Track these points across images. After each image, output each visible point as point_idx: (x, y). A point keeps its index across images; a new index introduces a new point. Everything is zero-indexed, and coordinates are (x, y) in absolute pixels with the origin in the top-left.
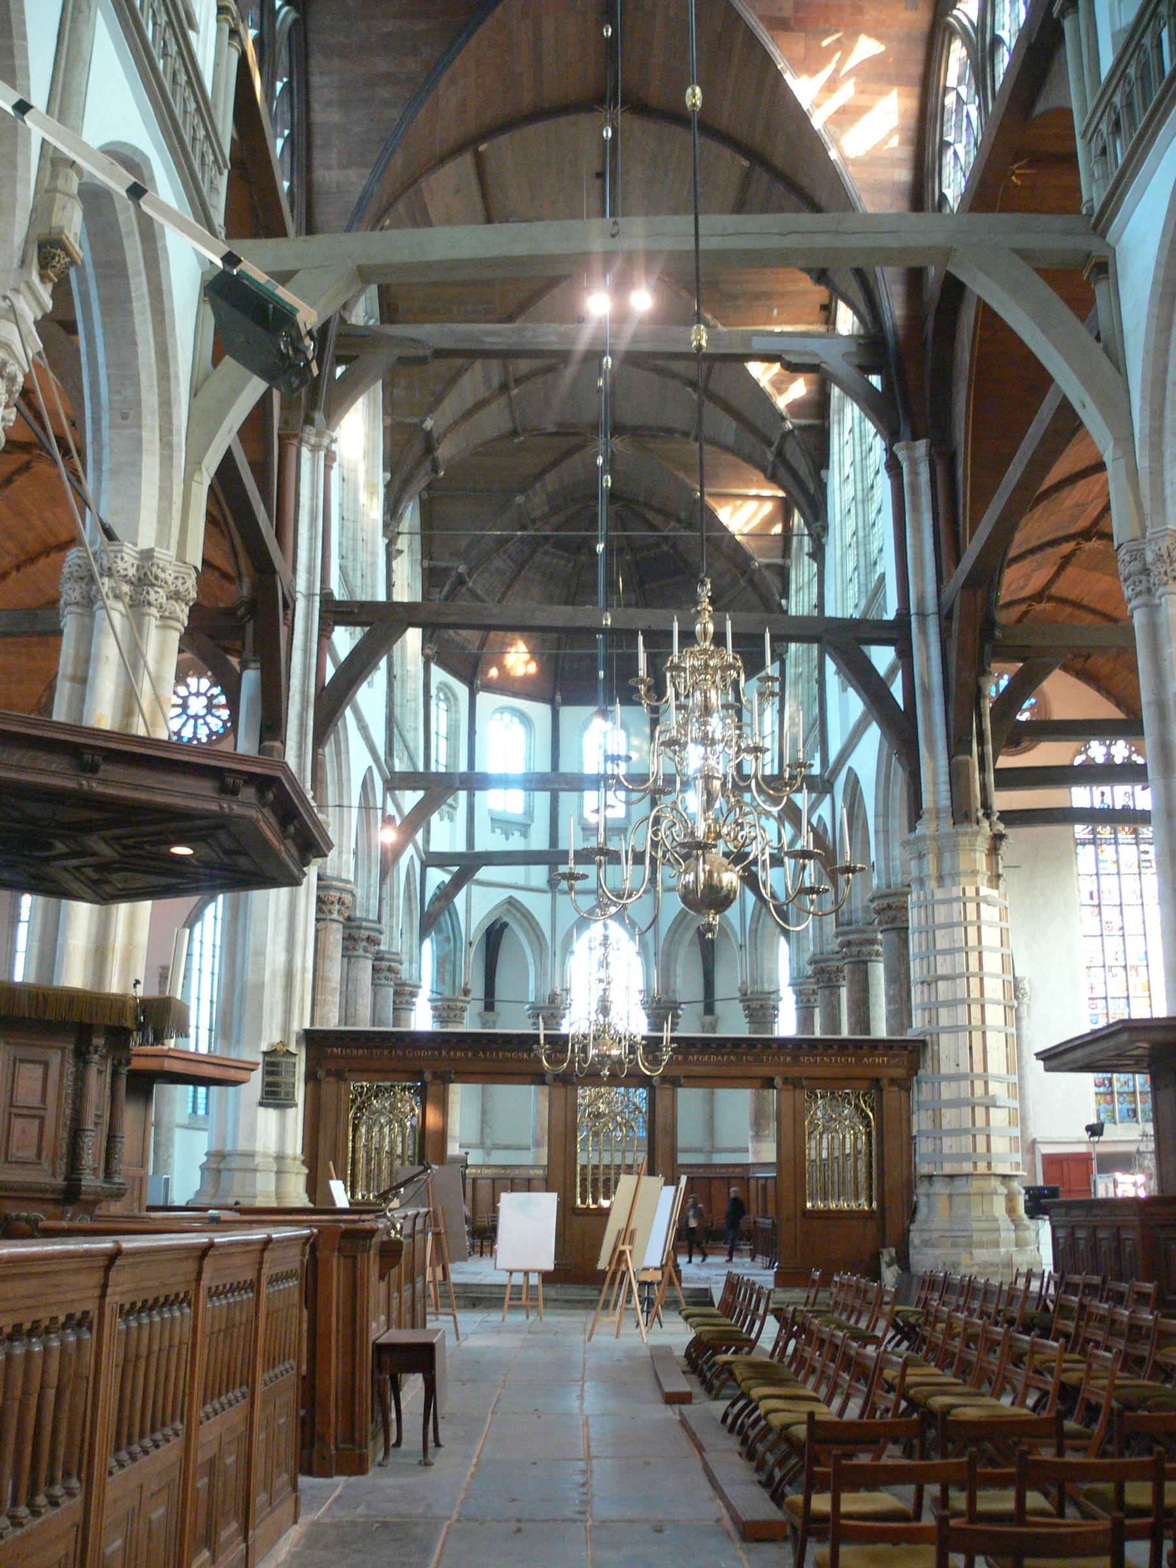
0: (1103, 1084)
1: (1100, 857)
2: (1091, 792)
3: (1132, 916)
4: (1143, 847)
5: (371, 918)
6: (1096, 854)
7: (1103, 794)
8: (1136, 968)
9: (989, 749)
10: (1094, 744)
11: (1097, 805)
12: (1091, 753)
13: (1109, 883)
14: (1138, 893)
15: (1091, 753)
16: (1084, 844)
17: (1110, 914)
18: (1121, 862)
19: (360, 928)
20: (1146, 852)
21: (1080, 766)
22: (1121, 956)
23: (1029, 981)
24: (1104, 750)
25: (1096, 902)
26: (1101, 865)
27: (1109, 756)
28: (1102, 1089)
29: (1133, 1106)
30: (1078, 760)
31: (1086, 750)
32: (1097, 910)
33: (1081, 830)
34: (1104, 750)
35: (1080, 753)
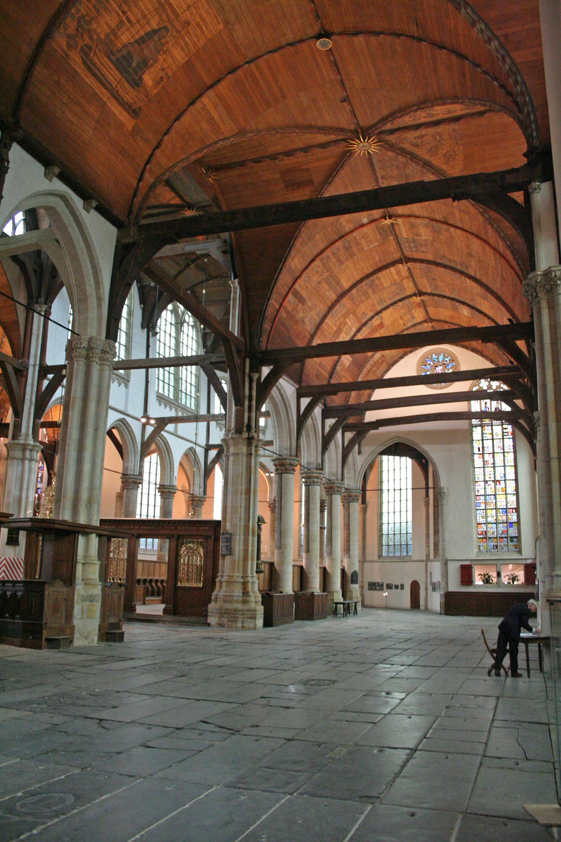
0: (482, 534)
1: (484, 432)
2: (480, 403)
3: (499, 458)
4: (504, 426)
5: (135, 474)
6: (482, 431)
7: (486, 403)
8: (499, 481)
9: (254, 403)
10: (483, 381)
11: (483, 409)
12: (481, 385)
13: (489, 444)
14: (502, 447)
15: (481, 385)
16: (476, 427)
17: (487, 457)
18: (494, 434)
19: (129, 478)
20: (506, 429)
21: (476, 391)
22: (492, 476)
23: (447, 489)
24: (487, 383)
25: (481, 452)
26: (484, 435)
27: (490, 387)
28: (481, 536)
29: (496, 544)
30: (475, 389)
31: (479, 384)
32: (481, 456)
33: (475, 422)
34: (487, 383)
35: (475, 386)
